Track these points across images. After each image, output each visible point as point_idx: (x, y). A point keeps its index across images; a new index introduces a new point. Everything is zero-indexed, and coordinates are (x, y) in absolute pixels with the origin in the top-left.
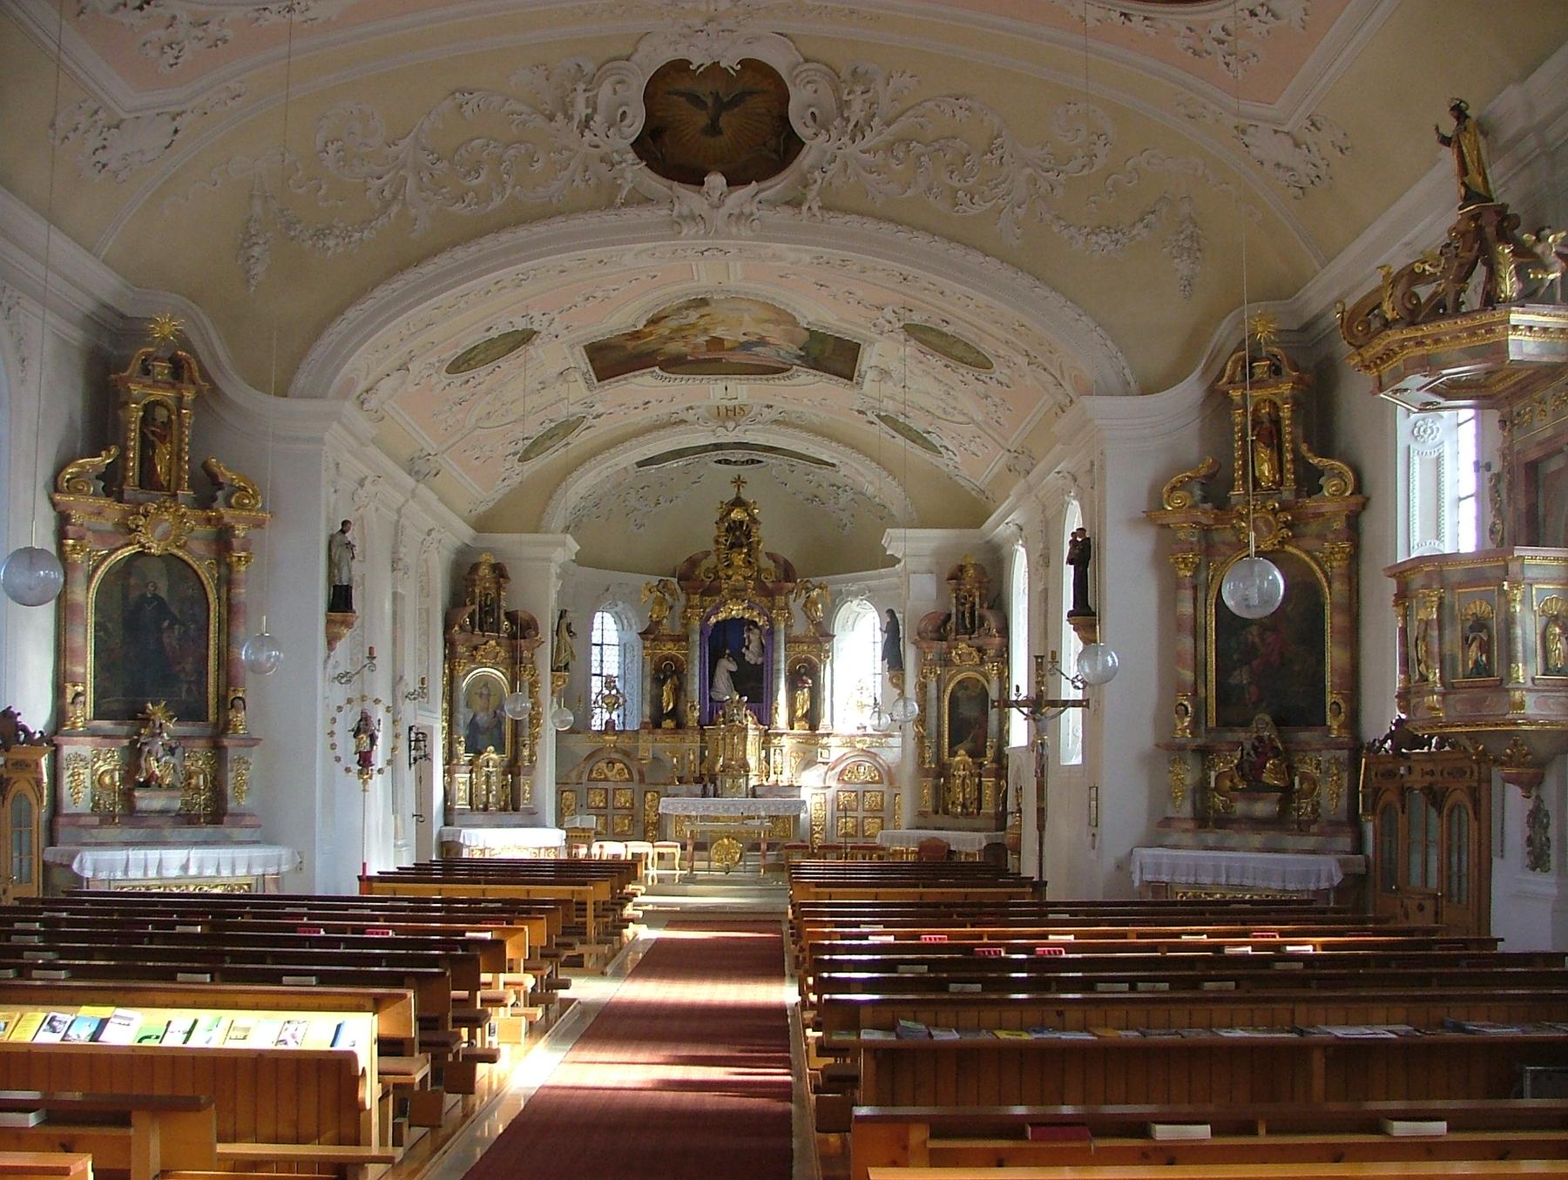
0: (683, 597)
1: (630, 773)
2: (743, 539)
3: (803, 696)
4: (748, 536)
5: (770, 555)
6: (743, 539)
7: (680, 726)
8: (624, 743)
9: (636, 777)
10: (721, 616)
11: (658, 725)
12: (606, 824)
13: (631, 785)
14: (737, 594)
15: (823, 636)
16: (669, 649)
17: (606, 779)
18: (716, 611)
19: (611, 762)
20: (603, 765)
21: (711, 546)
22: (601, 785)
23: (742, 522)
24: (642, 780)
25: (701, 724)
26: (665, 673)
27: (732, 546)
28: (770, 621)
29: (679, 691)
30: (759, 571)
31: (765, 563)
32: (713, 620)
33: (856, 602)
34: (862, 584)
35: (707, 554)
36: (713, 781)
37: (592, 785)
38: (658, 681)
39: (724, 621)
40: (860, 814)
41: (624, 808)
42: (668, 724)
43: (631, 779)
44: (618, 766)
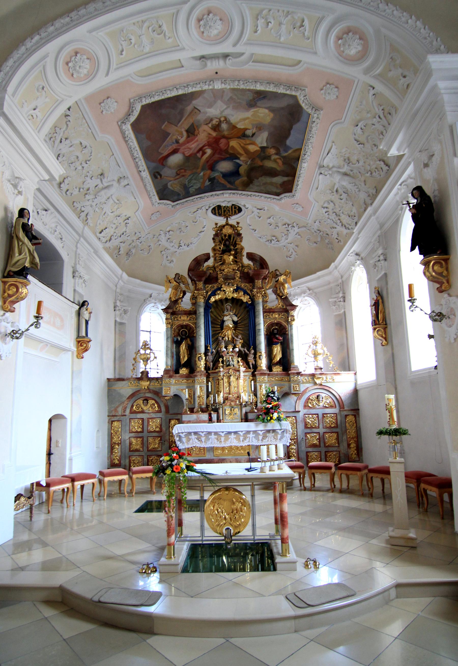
0: (192, 287)
1: (159, 406)
2: (232, 247)
3: (277, 350)
4: (235, 244)
5: (251, 256)
6: (232, 247)
7: (192, 370)
8: (155, 386)
9: (163, 409)
10: (217, 297)
11: (177, 372)
12: (142, 443)
13: (159, 415)
14: (228, 279)
15: (287, 307)
16: (184, 320)
17: (143, 412)
18: (214, 294)
19: (146, 400)
20: (140, 402)
21: (212, 254)
22: (140, 416)
23: (230, 236)
24: (167, 411)
25: (207, 368)
26: (182, 336)
27: (224, 252)
28: (252, 298)
29: (192, 349)
30: (243, 266)
31: (246, 261)
32: (213, 299)
33: (299, 299)
34: (304, 287)
35: (207, 257)
36: (216, 410)
37: (133, 416)
38: (178, 344)
39: (221, 300)
40: (321, 430)
41: (155, 432)
42: (184, 371)
43: (160, 411)
44: (151, 402)
